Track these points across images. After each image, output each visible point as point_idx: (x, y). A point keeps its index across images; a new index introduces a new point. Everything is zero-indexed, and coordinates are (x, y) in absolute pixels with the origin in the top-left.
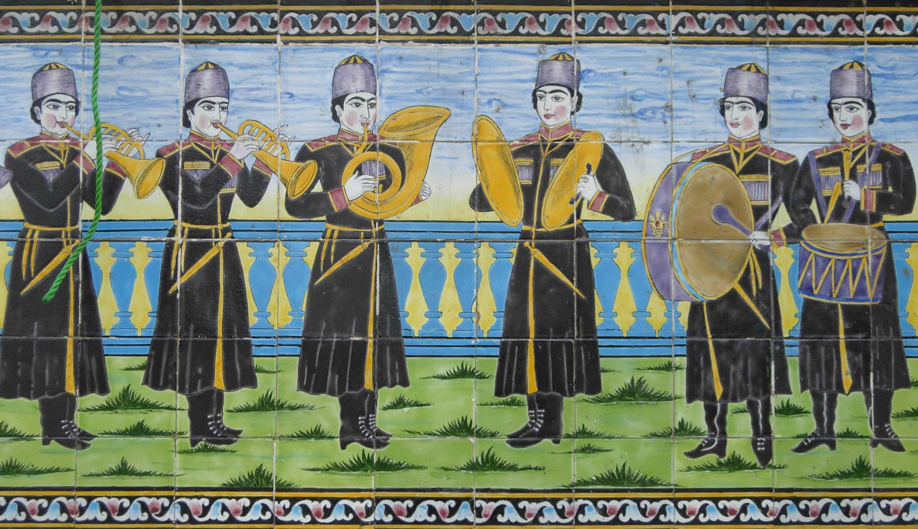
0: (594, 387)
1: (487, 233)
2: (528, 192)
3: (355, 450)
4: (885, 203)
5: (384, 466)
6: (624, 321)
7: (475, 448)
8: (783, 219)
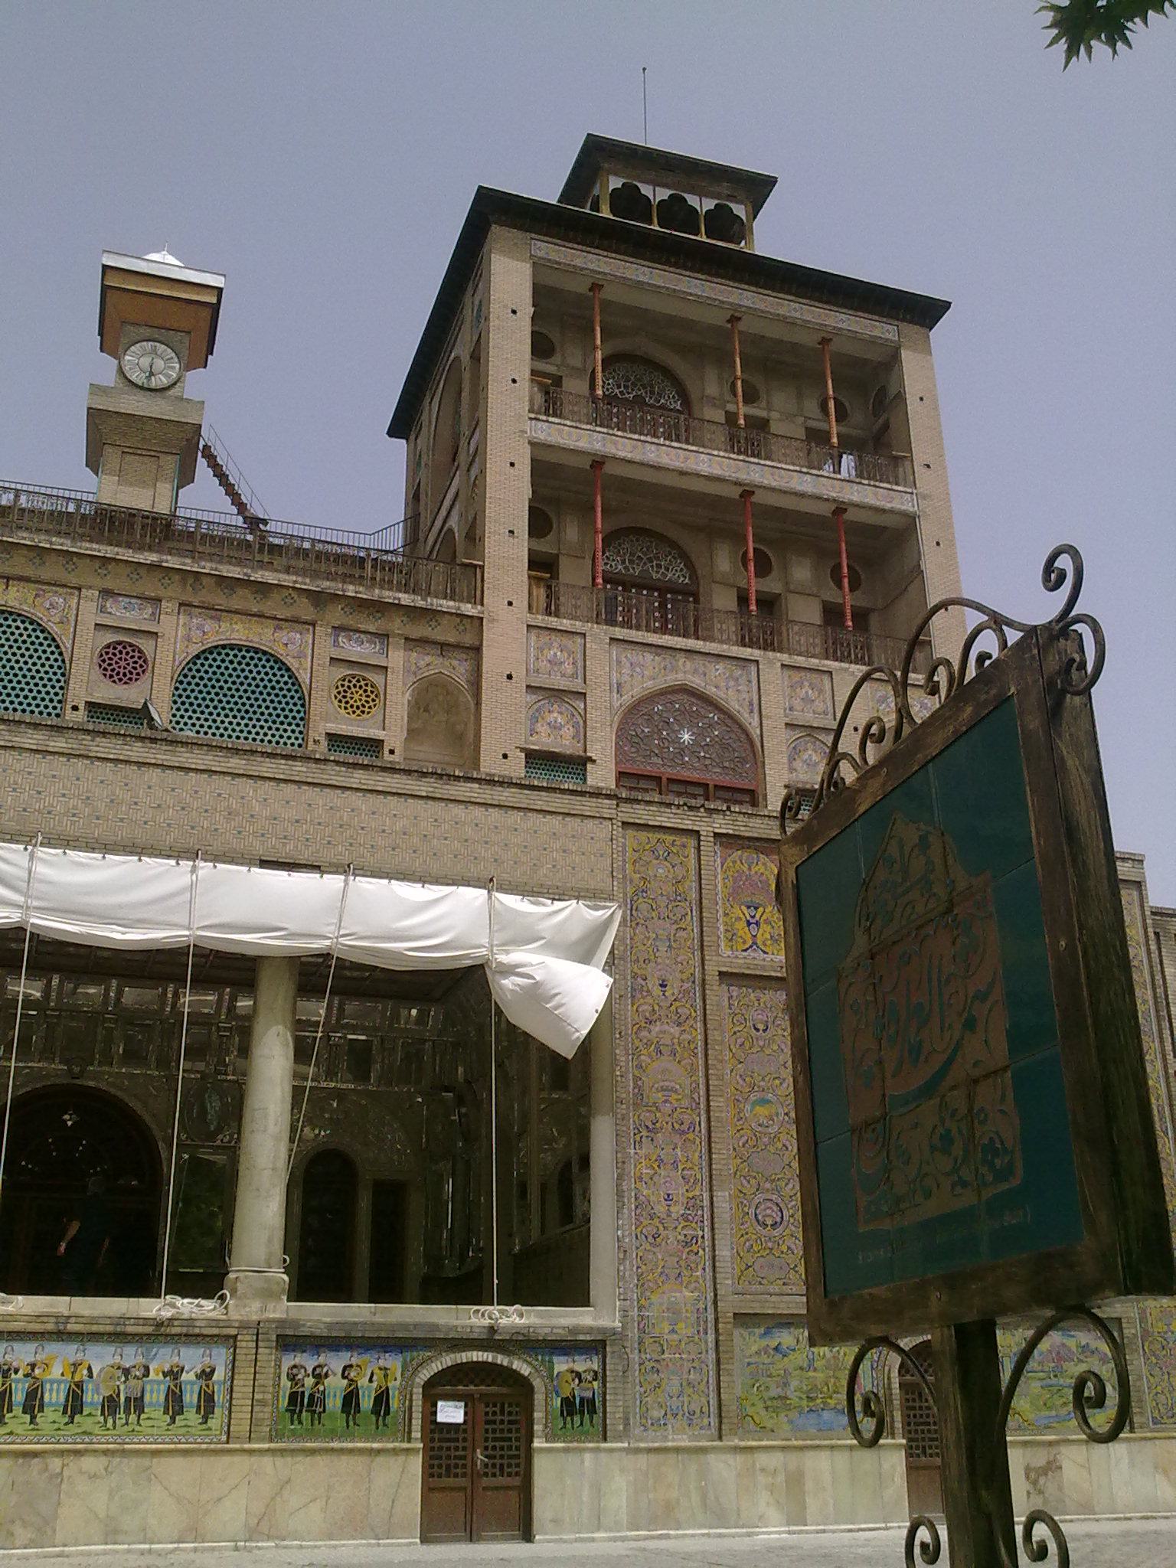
0: (82, 1413)
1: (63, 1381)
2: (73, 1373)
3: (32, 1426)
4: (144, 1376)
5: (38, 1430)
6: (89, 1400)
7: (56, 1426)
8: (123, 1379)
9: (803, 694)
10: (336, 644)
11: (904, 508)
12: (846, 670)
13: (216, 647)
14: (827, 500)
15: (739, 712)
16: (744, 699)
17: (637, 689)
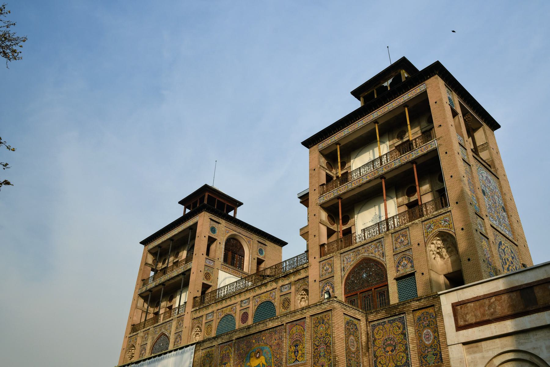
9: (399, 241)
10: (281, 291)
11: (432, 148)
12: (414, 223)
13: (260, 305)
14: (404, 164)
15: (379, 259)
16: (381, 253)
17: (349, 268)
